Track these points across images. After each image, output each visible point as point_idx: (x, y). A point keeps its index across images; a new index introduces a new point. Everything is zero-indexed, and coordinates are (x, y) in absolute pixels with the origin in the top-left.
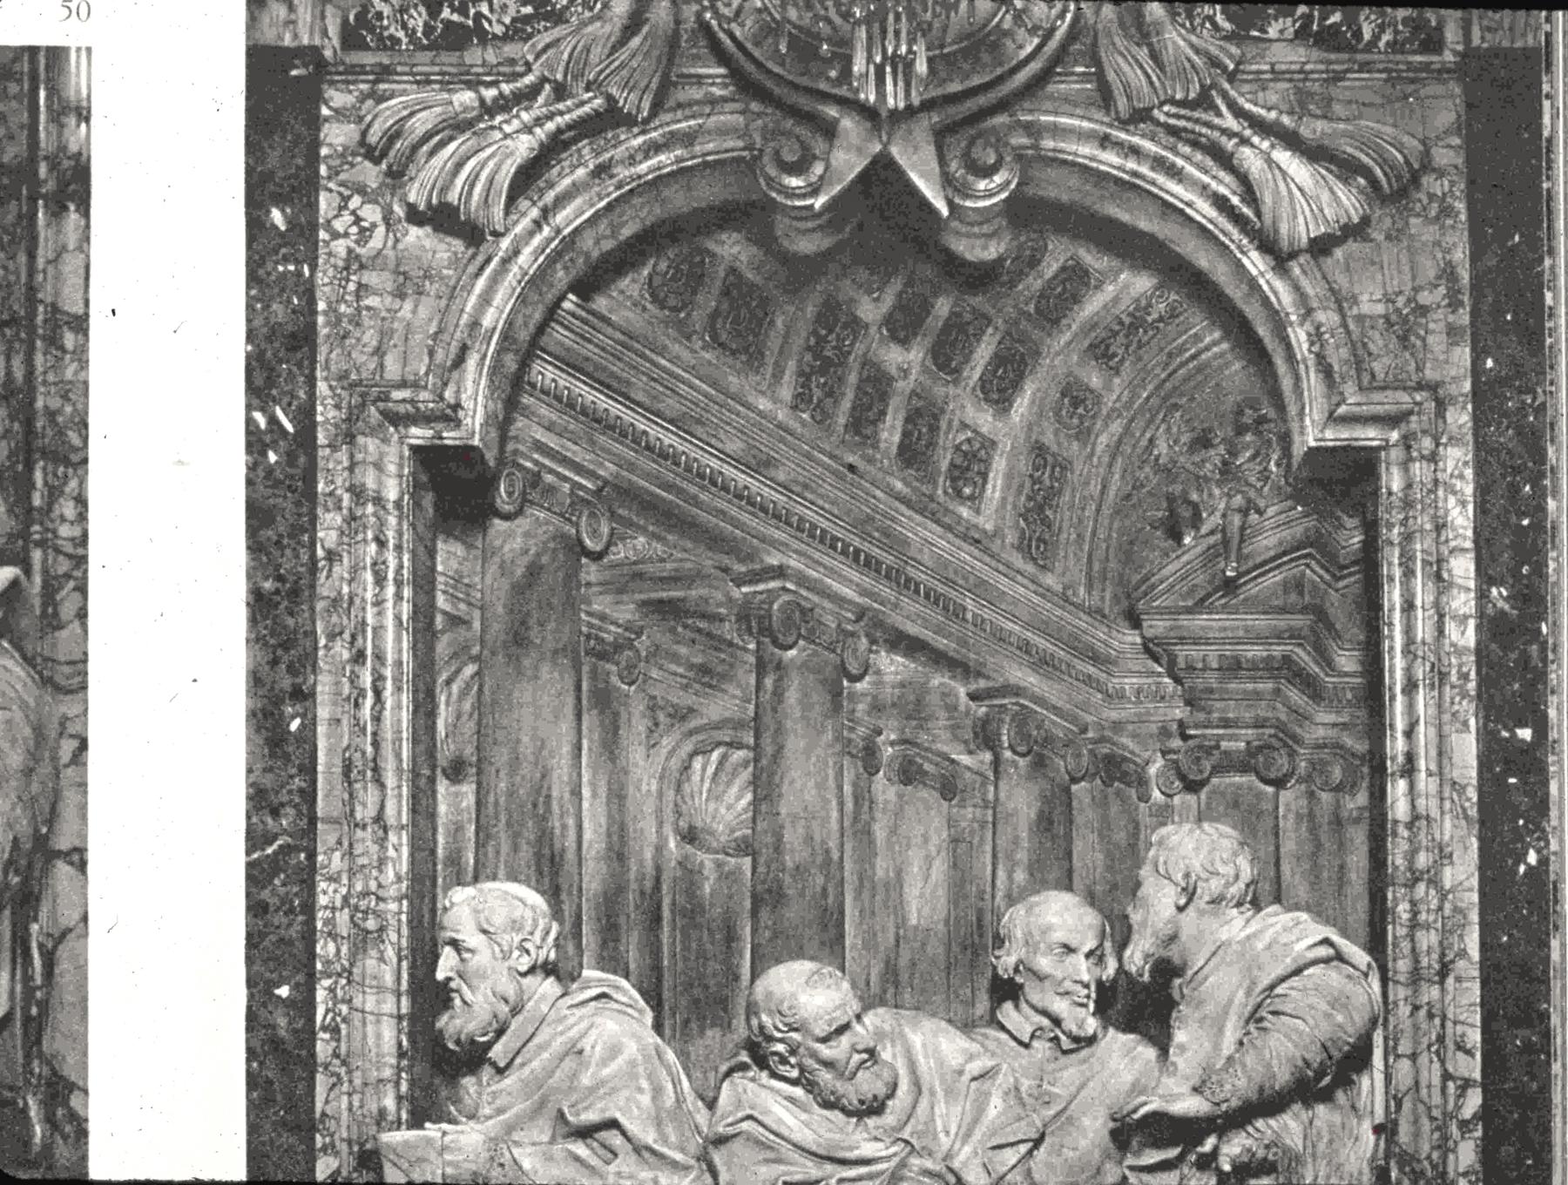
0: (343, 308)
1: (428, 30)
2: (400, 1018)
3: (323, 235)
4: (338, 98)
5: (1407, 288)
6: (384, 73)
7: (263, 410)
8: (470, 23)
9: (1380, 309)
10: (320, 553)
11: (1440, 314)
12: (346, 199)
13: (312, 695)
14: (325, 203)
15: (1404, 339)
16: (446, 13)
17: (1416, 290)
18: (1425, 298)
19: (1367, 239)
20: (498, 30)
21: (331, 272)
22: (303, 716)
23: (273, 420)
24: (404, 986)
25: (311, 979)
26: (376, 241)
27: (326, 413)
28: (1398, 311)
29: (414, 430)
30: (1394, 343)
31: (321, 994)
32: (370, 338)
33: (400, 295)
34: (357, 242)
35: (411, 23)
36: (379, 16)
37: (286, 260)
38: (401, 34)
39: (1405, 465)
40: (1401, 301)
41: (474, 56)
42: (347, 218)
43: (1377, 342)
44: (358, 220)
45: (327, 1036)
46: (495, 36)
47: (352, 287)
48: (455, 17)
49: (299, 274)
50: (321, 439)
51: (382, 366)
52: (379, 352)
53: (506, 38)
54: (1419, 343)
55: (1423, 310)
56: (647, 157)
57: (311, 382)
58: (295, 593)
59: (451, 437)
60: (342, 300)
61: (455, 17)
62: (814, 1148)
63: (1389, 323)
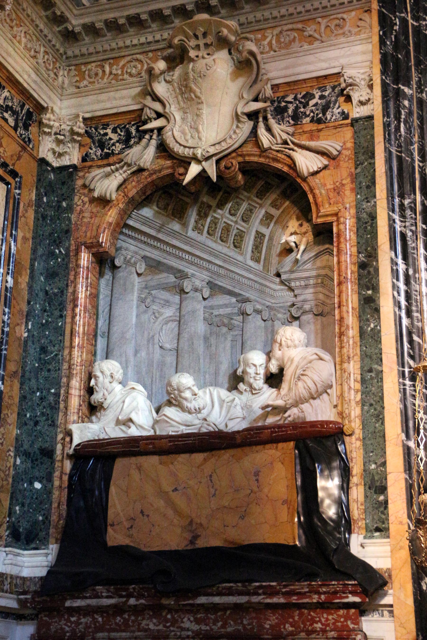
0: (78, 223)
1: (101, 155)
2: (80, 396)
3: (75, 206)
4: (81, 174)
5: (339, 180)
6: (90, 167)
7: (58, 249)
8: (110, 152)
9: (332, 186)
10: (69, 282)
11: (348, 185)
12: (80, 197)
13: (65, 315)
14: (76, 198)
15: (338, 193)
16: (105, 150)
17: (342, 180)
18: (344, 182)
19: (329, 169)
20: (117, 152)
21: (76, 214)
22: (62, 322)
23: (60, 251)
24: (82, 388)
25: (60, 388)
26: (87, 206)
27: (73, 248)
28: (337, 186)
29: (93, 250)
30: (336, 194)
31: (62, 392)
32: (84, 228)
33: (91, 218)
34: (83, 207)
35: (97, 154)
36: (90, 153)
37: (65, 213)
38: (95, 157)
39: (338, 225)
40: (337, 184)
41: (112, 160)
42: (81, 201)
43: (331, 195)
44: (83, 201)
45: (62, 402)
46: (116, 154)
47: (81, 217)
48: (107, 151)
49: (68, 216)
50: (71, 254)
51: (86, 236)
52: (86, 232)
53: (119, 154)
54: (343, 194)
55: (343, 185)
56: (150, 177)
57: (69, 241)
58: (62, 292)
59: (101, 250)
60: (78, 221)
61: (107, 151)
62: (180, 421)
63: (335, 190)
